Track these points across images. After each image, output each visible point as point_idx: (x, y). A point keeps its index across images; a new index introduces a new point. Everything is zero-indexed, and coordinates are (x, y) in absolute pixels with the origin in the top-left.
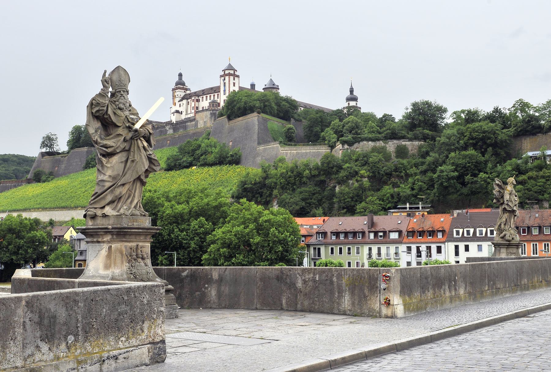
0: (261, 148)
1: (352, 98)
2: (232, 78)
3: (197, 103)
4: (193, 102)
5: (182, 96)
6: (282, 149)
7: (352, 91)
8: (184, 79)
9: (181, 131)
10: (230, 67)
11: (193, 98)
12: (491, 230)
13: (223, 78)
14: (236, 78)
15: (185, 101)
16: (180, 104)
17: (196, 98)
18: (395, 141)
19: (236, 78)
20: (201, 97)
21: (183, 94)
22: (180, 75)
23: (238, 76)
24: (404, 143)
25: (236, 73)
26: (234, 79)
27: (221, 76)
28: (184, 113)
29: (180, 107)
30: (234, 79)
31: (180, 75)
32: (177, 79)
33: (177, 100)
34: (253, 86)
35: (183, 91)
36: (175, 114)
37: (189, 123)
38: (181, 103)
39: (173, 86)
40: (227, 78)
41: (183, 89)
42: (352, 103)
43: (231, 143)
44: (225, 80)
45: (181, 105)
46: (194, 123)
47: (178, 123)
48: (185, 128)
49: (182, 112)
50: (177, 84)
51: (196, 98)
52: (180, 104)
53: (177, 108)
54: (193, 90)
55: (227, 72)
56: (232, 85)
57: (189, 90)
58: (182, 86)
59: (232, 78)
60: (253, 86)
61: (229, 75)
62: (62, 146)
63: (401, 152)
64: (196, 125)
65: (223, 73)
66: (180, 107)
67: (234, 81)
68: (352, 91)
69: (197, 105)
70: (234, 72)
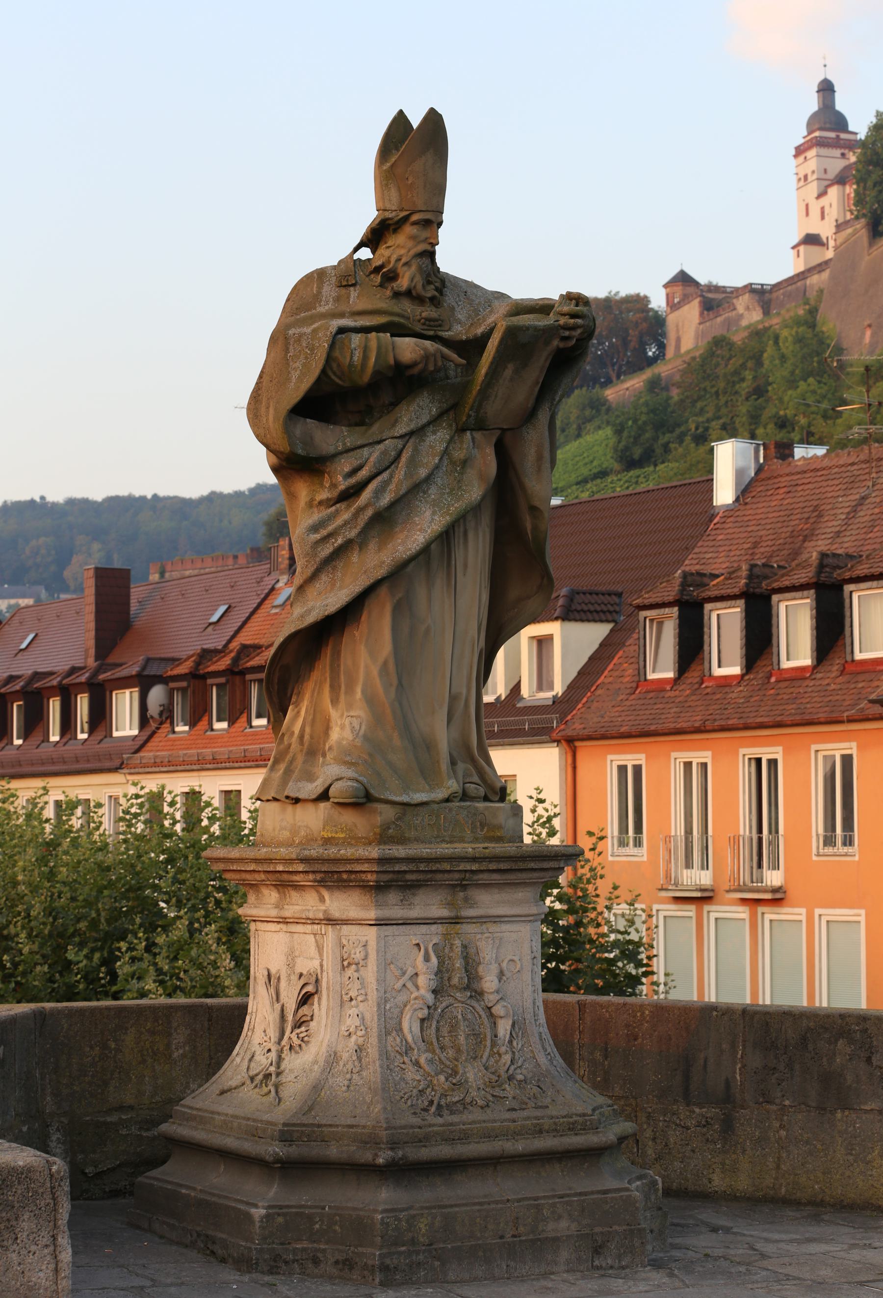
5: (832, 175)
8: (840, 105)
16: (823, 209)
21: (836, 165)
22: (826, 89)
29: (823, 218)
31: (826, 89)
32: (812, 104)
35: (837, 152)
36: (802, 248)
38: (824, 201)
39: (799, 134)
41: (836, 144)
43: (868, 333)
45: (827, 211)
49: (827, 238)
50: (813, 123)
52: (823, 209)
58: (832, 135)
66: (823, 218)
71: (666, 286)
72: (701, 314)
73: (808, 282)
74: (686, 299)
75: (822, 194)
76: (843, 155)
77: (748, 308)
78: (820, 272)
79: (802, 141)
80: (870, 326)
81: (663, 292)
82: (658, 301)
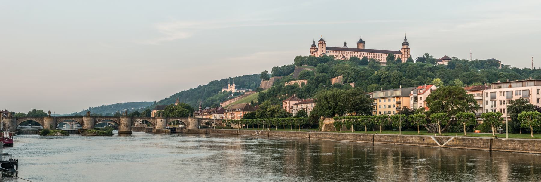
1: (406, 43)
2: (321, 45)
7: (405, 39)
10: (322, 40)
14: (324, 45)
18: (302, 81)
19: (324, 45)
24: (304, 81)
26: (323, 45)
30: (323, 45)
34: (345, 44)
39: (311, 47)
41: (314, 48)
42: (405, 47)
50: (312, 46)
55: (320, 42)
56: (321, 48)
59: (321, 45)
60: (345, 44)
61: (320, 43)
63: (303, 84)
68: (405, 39)
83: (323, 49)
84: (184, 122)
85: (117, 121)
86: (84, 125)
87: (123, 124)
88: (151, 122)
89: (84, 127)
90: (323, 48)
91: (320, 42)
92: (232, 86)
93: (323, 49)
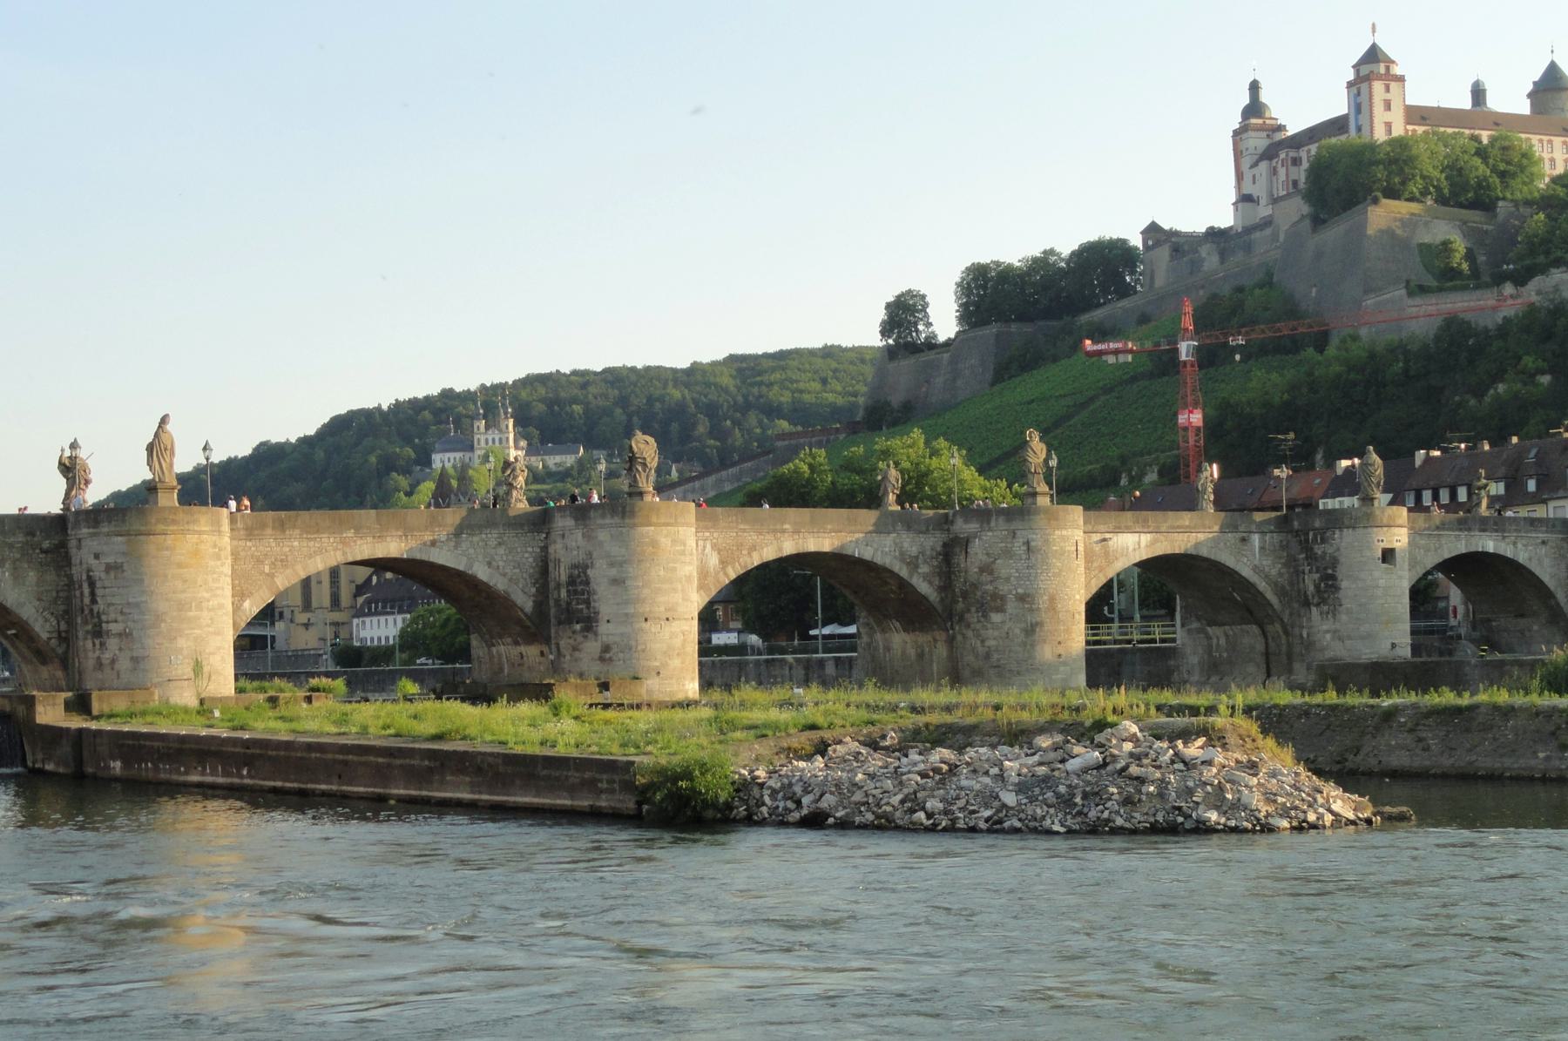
0: (1370, 302)
3: (1293, 169)
4: (1283, 166)
5: (1260, 151)
6: (1410, 302)
8: (1264, 97)
9: (1240, 256)
10: (1373, 55)
11: (1282, 155)
12: (1555, 507)
13: (1354, 90)
15: (1264, 165)
16: (1254, 177)
17: (1293, 154)
19: (1393, 85)
20: (1306, 148)
22: (1254, 87)
23: (1401, 79)
25: (1397, 70)
26: (1388, 89)
27: (1350, 85)
28: (1263, 202)
29: (1254, 183)
30: (1388, 89)
31: (1254, 87)
32: (1246, 100)
33: (1246, 162)
34: (1478, 93)
35: (1265, 134)
36: (1240, 205)
37: (1257, 235)
38: (1255, 170)
39: (1235, 121)
40: (1364, 86)
43: (1314, 290)
44: (1359, 94)
46: (1268, 231)
47: (1248, 230)
48: (1248, 248)
51: (1293, 154)
52: (1254, 177)
53: (1248, 189)
54: (1292, 130)
55: (1365, 70)
57: (1281, 128)
58: (1260, 121)
60: (1478, 93)
62: (944, 322)
64: (1275, 236)
65: (1351, 76)
66: (1254, 183)
67: (1388, 96)
69: (1293, 177)
70: (1388, 68)
71: (1142, 233)
72: (1171, 256)
73: (1253, 237)
74: (1157, 244)
75: (1255, 165)
76: (1268, 136)
77: (1209, 254)
78: (1261, 230)
79: (1238, 126)
80: (1315, 286)
81: (1140, 238)
82: (1136, 241)
83: (1388, 117)
84: (1537, 571)
85: (913, 564)
86: (589, 623)
87: (1011, 607)
88: (1246, 572)
89: (592, 647)
90: (1388, 105)
91: (1365, 70)
92: (493, 435)
93: (1388, 117)
